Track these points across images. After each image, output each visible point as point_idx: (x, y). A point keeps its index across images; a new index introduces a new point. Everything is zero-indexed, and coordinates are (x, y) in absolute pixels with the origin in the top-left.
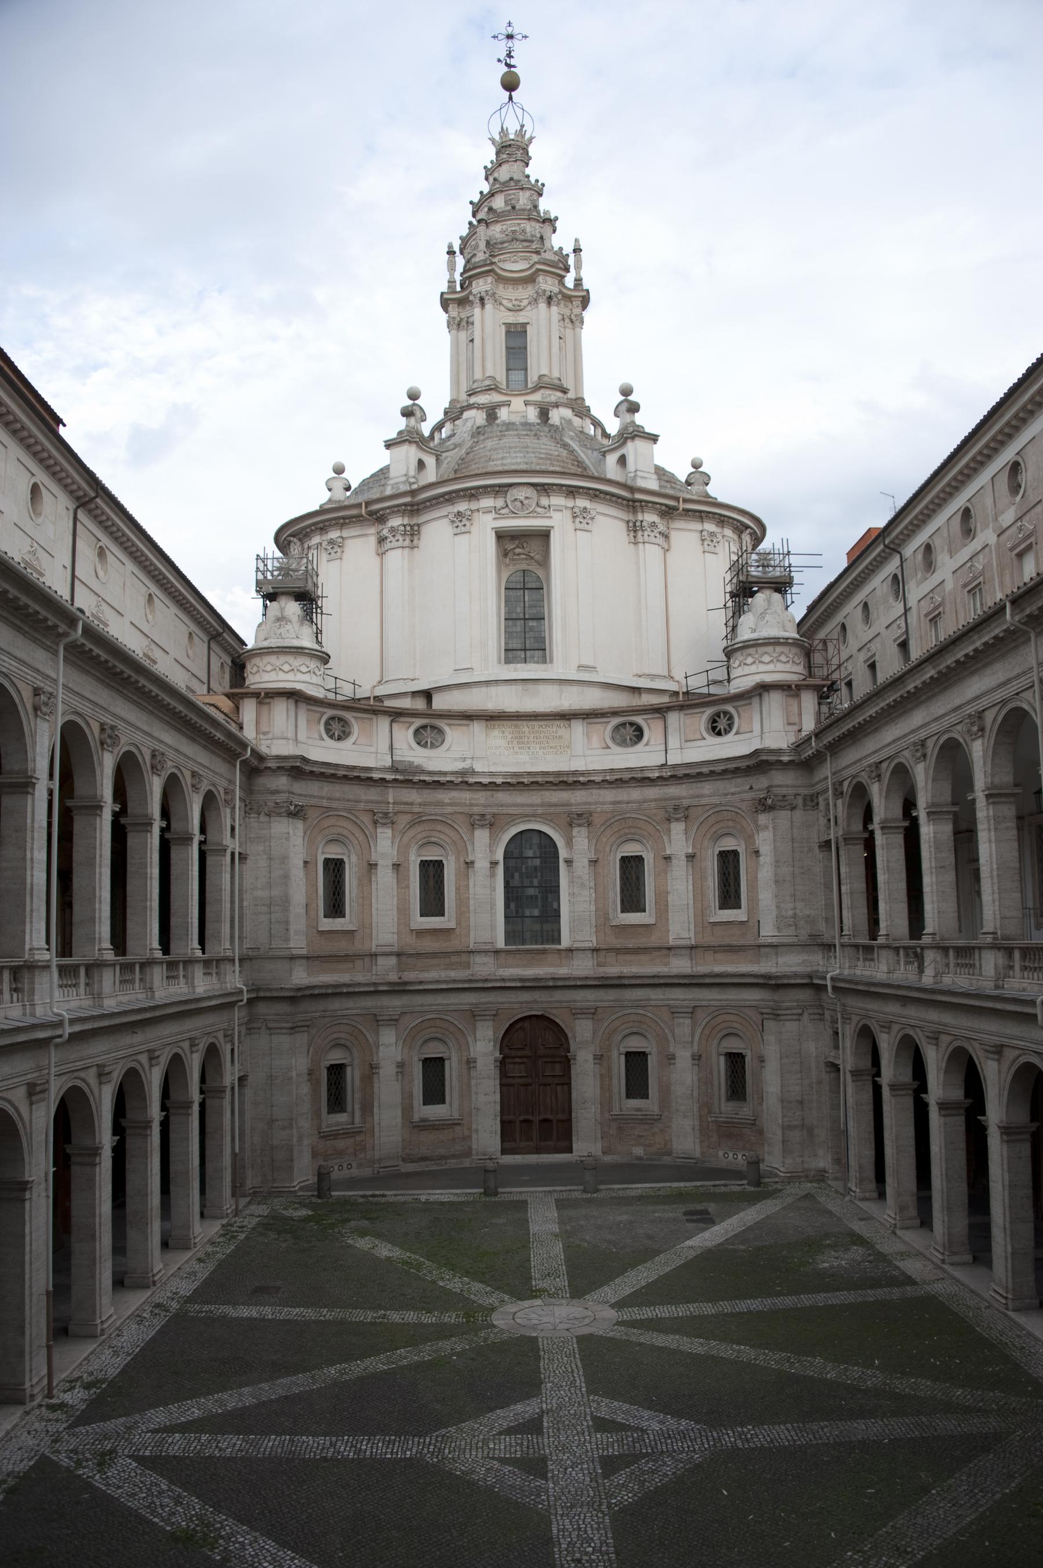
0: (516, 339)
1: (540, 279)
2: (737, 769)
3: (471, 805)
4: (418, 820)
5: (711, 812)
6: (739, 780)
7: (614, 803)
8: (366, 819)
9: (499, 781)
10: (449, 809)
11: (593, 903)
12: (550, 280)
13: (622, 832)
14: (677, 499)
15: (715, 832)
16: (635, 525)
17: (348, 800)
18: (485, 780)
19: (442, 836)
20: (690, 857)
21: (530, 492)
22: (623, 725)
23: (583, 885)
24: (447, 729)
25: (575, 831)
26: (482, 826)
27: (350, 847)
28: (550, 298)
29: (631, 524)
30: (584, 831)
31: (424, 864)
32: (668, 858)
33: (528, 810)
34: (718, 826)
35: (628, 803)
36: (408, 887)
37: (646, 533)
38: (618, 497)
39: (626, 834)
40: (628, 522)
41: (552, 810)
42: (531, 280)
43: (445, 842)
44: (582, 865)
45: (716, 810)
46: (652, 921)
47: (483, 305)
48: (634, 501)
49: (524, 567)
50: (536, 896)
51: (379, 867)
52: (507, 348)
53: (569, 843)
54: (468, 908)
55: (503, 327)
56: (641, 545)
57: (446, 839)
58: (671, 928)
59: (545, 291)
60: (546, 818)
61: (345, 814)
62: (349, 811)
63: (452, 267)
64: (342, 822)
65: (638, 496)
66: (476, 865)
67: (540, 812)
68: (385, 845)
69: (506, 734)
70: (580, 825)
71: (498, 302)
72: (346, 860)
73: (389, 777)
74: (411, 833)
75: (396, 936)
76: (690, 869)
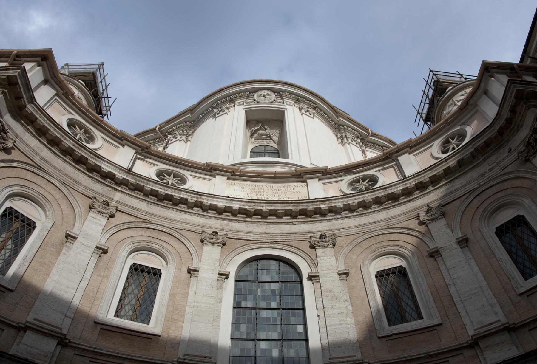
2: (487, 144)
3: (203, 226)
4: (140, 223)
5: (472, 198)
6: (493, 158)
7: (359, 226)
8: (82, 204)
9: (236, 206)
10: (179, 226)
11: (350, 315)
13: (374, 247)
14: (366, 130)
15: (484, 211)
17: (66, 175)
18: (221, 204)
19: (165, 245)
20: (464, 242)
21: (270, 92)
22: (357, 181)
23: (335, 298)
24: (190, 178)
25: (319, 251)
26: (213, 243)
27: (50, 213)
30: (329, 251)
31: (137, 269)
32: (434, 254)
33: (266, 238)
34: (484, 205)
35: (375, 223)
36: (107, 277)
37: (350, 140)
39: (378, 249)
41: (292, 238)
43: (168, 251)
44: (330, 278)
45: (477, 193)
46: (436, 321)
49: (266, 144)
50: (275, 319)
51: (76, 243)
53: (314, 263)
54: (183, 316)
56: (347, 145)
57: (170, 248)
58: (466, 321)
60: (286, 244)
61: (57, 183)
62: (64, 184)
64: (49, 188)
66: (200, 274)
67: (279, 239)
68: (93, 228)
69: (246, 189)
70: (324, 247)
72: (38, 224)
73: (120, 175)
74: (131, 233)
75: (68, 322)
76: (468, 254)
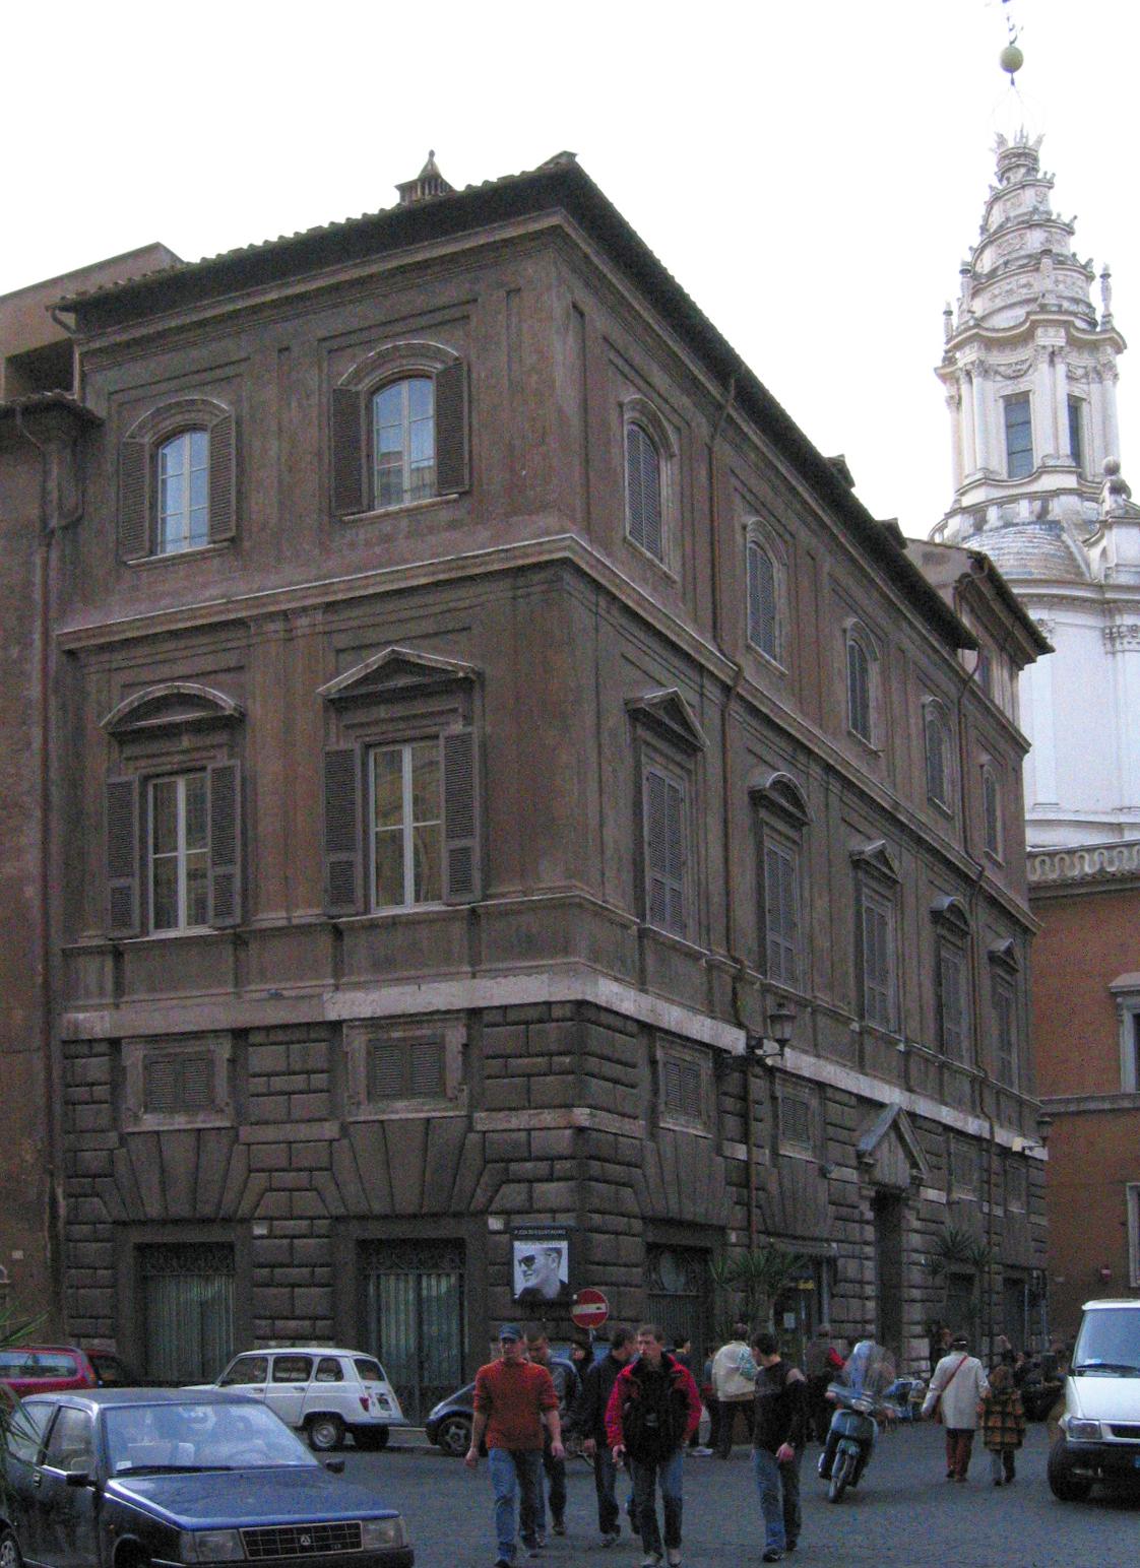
0: (1017, 408)
1: (1039, 331)
12: (1052, 331)
16: (1111, 633)
28: (1053, 353)
29: (1107, 631)
37: (1125, 641)
38: (1085, 600)
40: (1103, 630)
42: (1027, 337)
47: (971, 381)
48: (1108, 602)
52: (1009, 427)
55: (1001, 401)
59: (1044, 347)
63: (948, 325)
65: (1109, 595)
71: (986, 371)
